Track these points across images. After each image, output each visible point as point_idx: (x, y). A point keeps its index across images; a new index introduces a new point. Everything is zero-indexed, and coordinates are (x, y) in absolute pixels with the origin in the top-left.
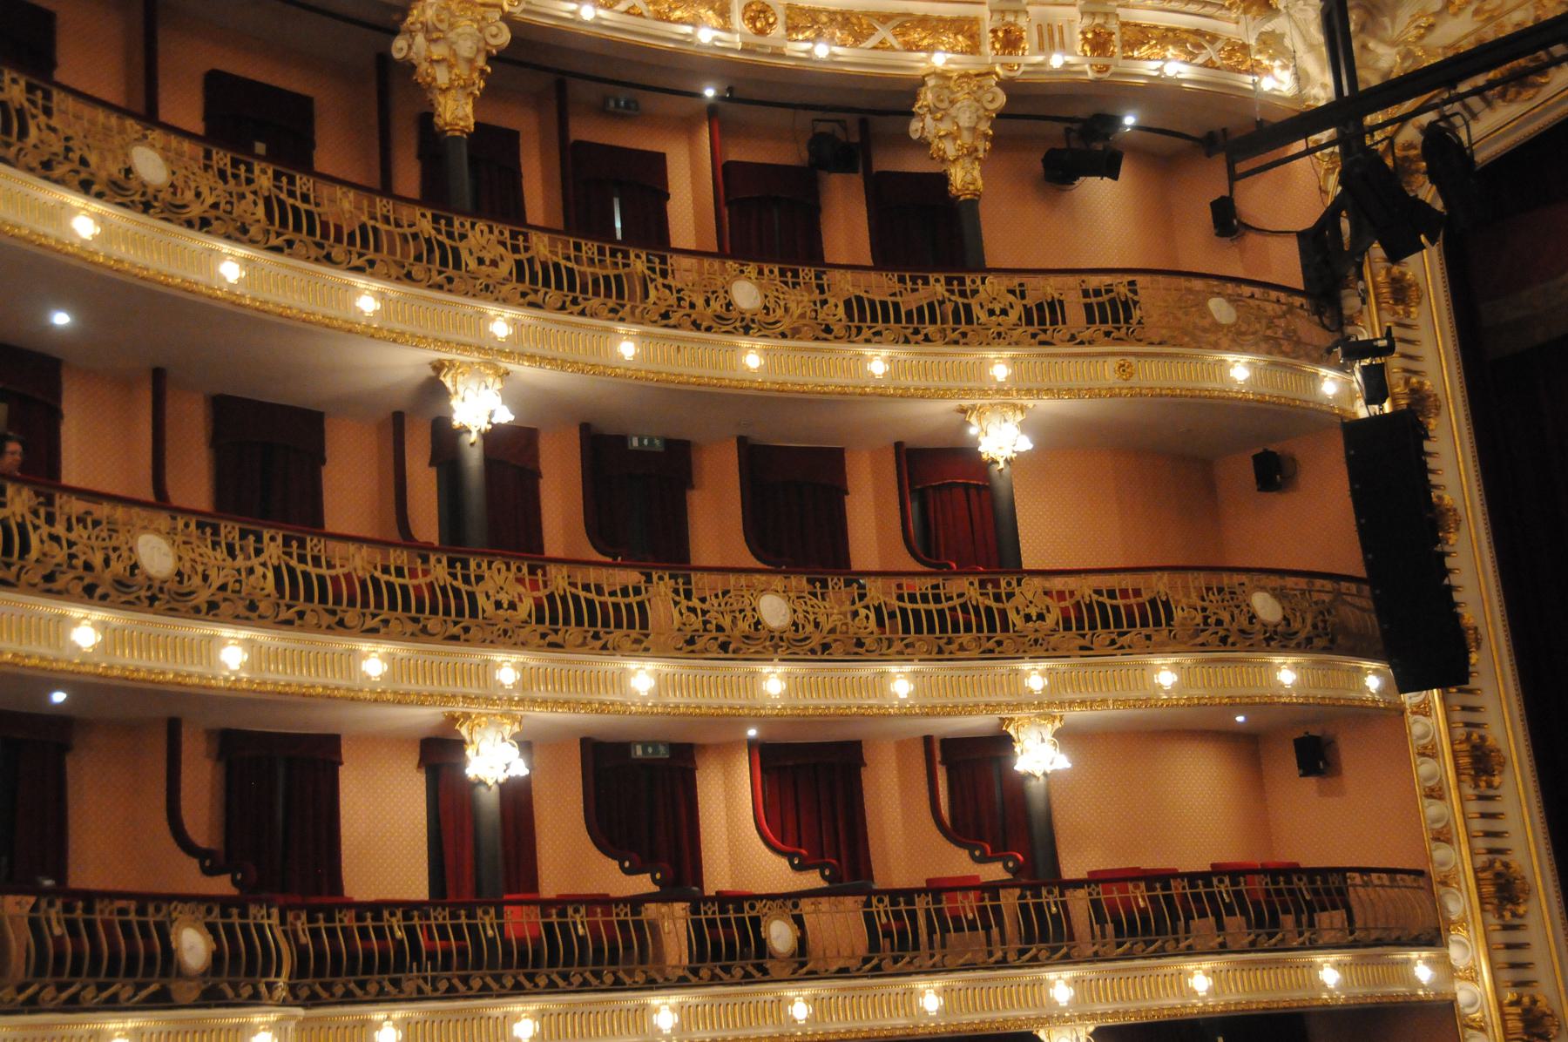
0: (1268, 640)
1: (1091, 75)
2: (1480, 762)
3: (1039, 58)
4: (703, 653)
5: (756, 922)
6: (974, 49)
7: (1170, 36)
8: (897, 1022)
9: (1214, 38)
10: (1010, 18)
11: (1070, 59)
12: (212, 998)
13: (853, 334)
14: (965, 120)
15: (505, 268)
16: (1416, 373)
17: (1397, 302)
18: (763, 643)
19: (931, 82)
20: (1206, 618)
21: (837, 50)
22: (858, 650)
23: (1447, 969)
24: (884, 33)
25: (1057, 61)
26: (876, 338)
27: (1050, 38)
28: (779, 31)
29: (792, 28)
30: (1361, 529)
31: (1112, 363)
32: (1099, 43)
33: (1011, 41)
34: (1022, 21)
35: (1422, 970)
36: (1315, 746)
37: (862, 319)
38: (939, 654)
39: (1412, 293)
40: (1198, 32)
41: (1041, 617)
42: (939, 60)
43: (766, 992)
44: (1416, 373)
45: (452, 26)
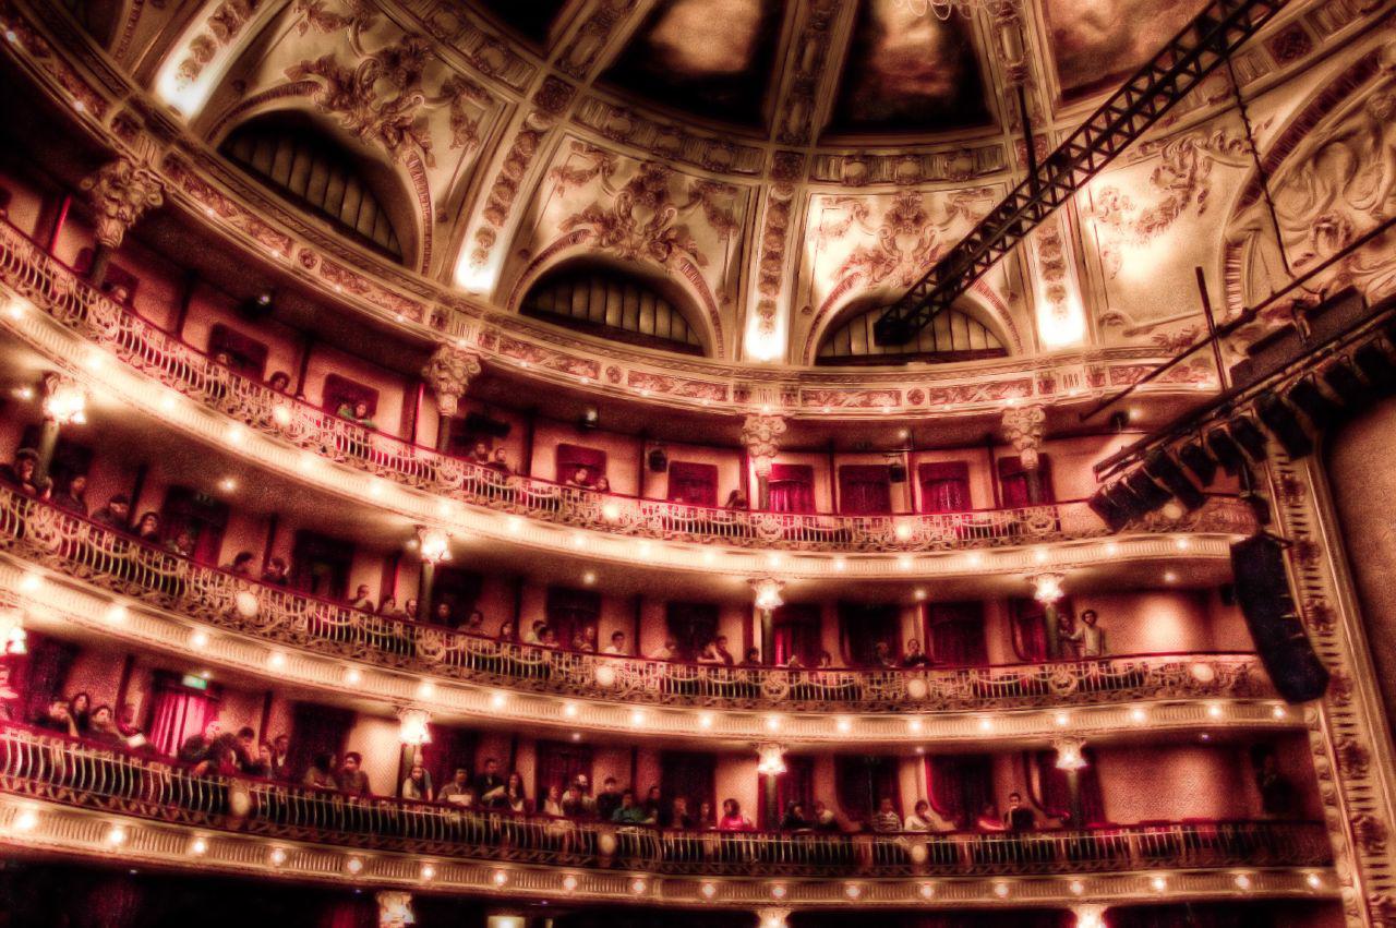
6: (1030, 393)
14: (1024, 428)
16: (1303, 532)
19: (1007, 413)
20: (1163, 682)
24: (982, 393)
27: (1070, 380)
32: (1096, 378)
33: (1047, 385)
44: (1303, 532)
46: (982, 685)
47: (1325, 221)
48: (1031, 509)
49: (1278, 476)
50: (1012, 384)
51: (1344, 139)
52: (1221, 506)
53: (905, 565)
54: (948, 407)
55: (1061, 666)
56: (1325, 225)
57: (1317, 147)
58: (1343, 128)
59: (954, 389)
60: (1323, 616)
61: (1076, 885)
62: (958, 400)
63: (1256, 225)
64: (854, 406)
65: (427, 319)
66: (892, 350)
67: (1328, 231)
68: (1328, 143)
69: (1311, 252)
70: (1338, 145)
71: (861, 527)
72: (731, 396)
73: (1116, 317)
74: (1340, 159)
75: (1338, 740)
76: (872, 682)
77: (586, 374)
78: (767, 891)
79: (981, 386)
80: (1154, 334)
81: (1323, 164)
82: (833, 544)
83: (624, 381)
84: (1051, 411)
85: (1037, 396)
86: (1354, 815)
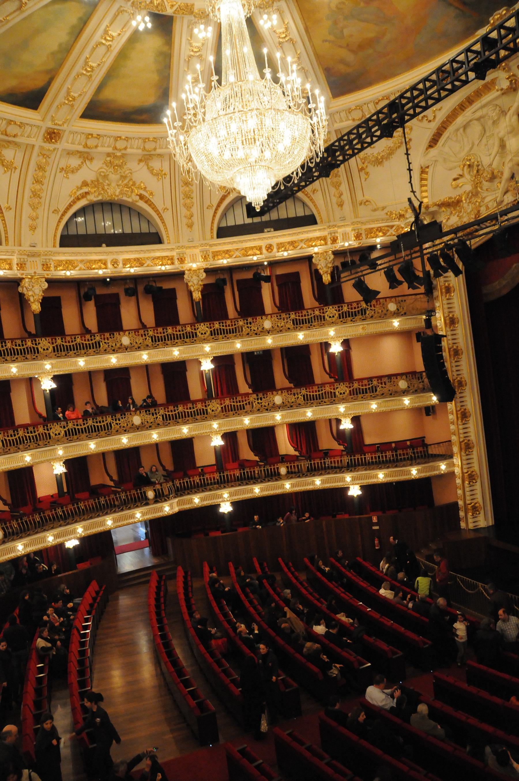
0: (404, 393)
1: (356, 246)
2: (464, 415)
3: (342, 244)
4: (262, 412)
5: (278, 468)
6: (326, 244)
7: (380, 229)
8: (310, 487)
9: (392, 227)
10: (333, 235)
11: (350, 242)
12: (156, 502)
13: (295, 329)
15: (208, 333)
17: (446, 293)
18: (276, 408)
21: (289, 252)
22: (299, 406)
23: (454, 465)
24: (302, 245)
25: (346, 244)
26: (301, 329)
27: (346, 237)
28: (275, 250)
29: (278, 249)
30: (425, 365)
31: (361, 327)
32: (358, 237)
33: (334, 240)
34: (337, 235)
35: (443, 467)
36: (429, 410)
37: (297, 324)
38: (320, 404)
39: (452, 289)
40: (388, 226)
41: (344, 393)
42: (316, 250)
43: (279, 483)
45: (192, 277)
46: (307, 395)
47: (467, 160)
48: (327, 307)
49: (442, 284)
50: (318, 238)
51: (478, 119)
52: (416, 300)
53: (269, 341)
54: (285, 254)
55: (342, 384)
56: (468, 163)
57: (465, 123)
58: (478, 114)
59: (289, 243)
60: (456, 353)
61: (348, 478)
62: (291, 247)
63: (434, 159)
64: (239, 257)
65: (15, 267)
66: (257, 220)
67: (469, 166)
68: (471, 121)
69: (461, 173)
70: (475, 122)
71: (247, 323)
72: (176, 262)
73: (367, 201)
74: (476, 129)
75: (458, 409)
76: (258, 399)
77: (100, 268)
78: (221, 496)
79: (302, 241)
80: (386, 211)
81: (468, 130)
82: (234, 334)
83: (121, 265)
84: (337, 254)
85: (331, 247)
86: (461, 440)
